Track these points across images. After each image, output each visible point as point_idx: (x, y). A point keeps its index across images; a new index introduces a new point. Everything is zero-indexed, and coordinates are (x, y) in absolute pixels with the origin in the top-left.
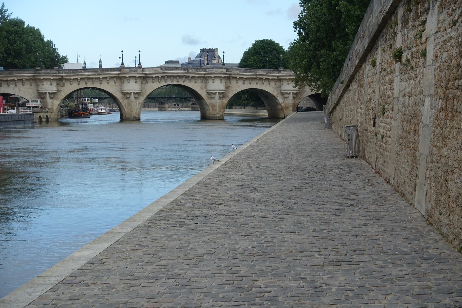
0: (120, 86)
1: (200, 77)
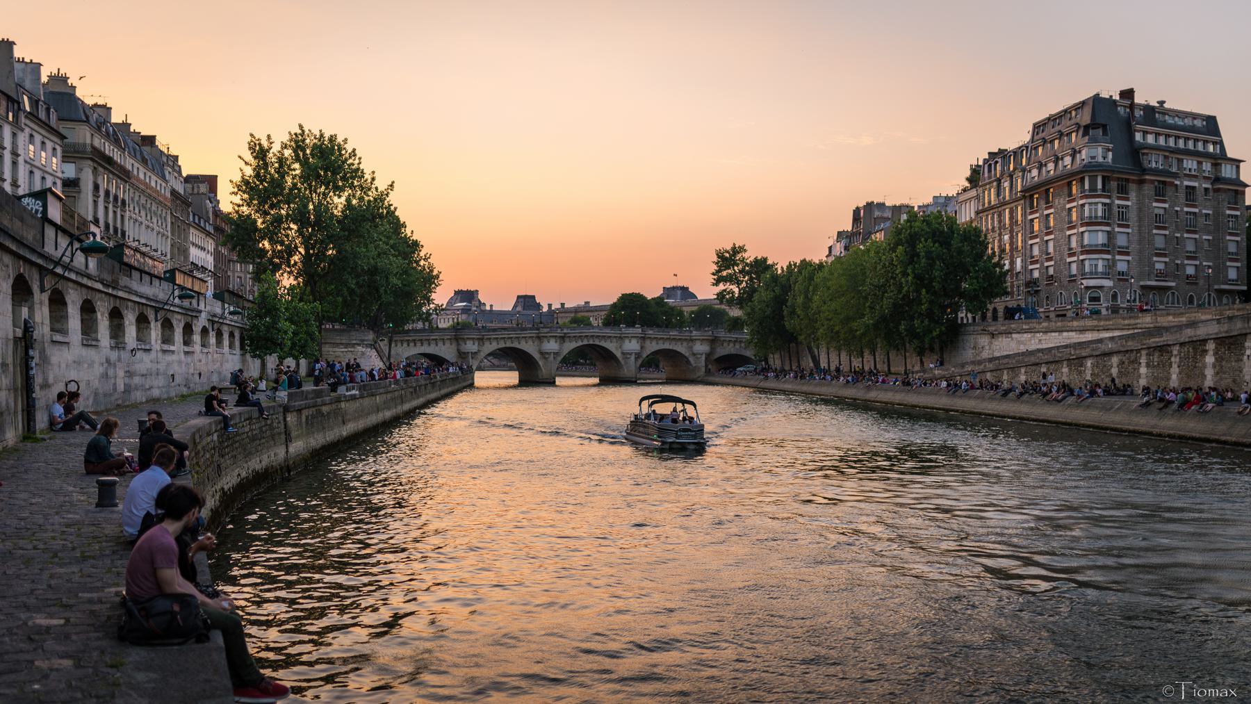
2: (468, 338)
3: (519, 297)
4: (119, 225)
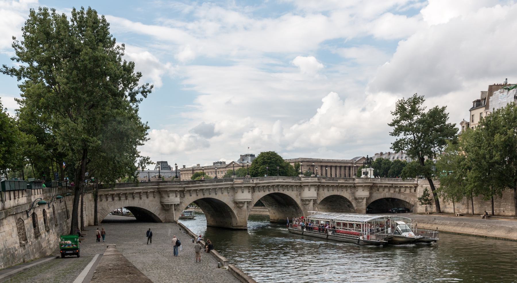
0: (232, 196)
2: (170, 191)
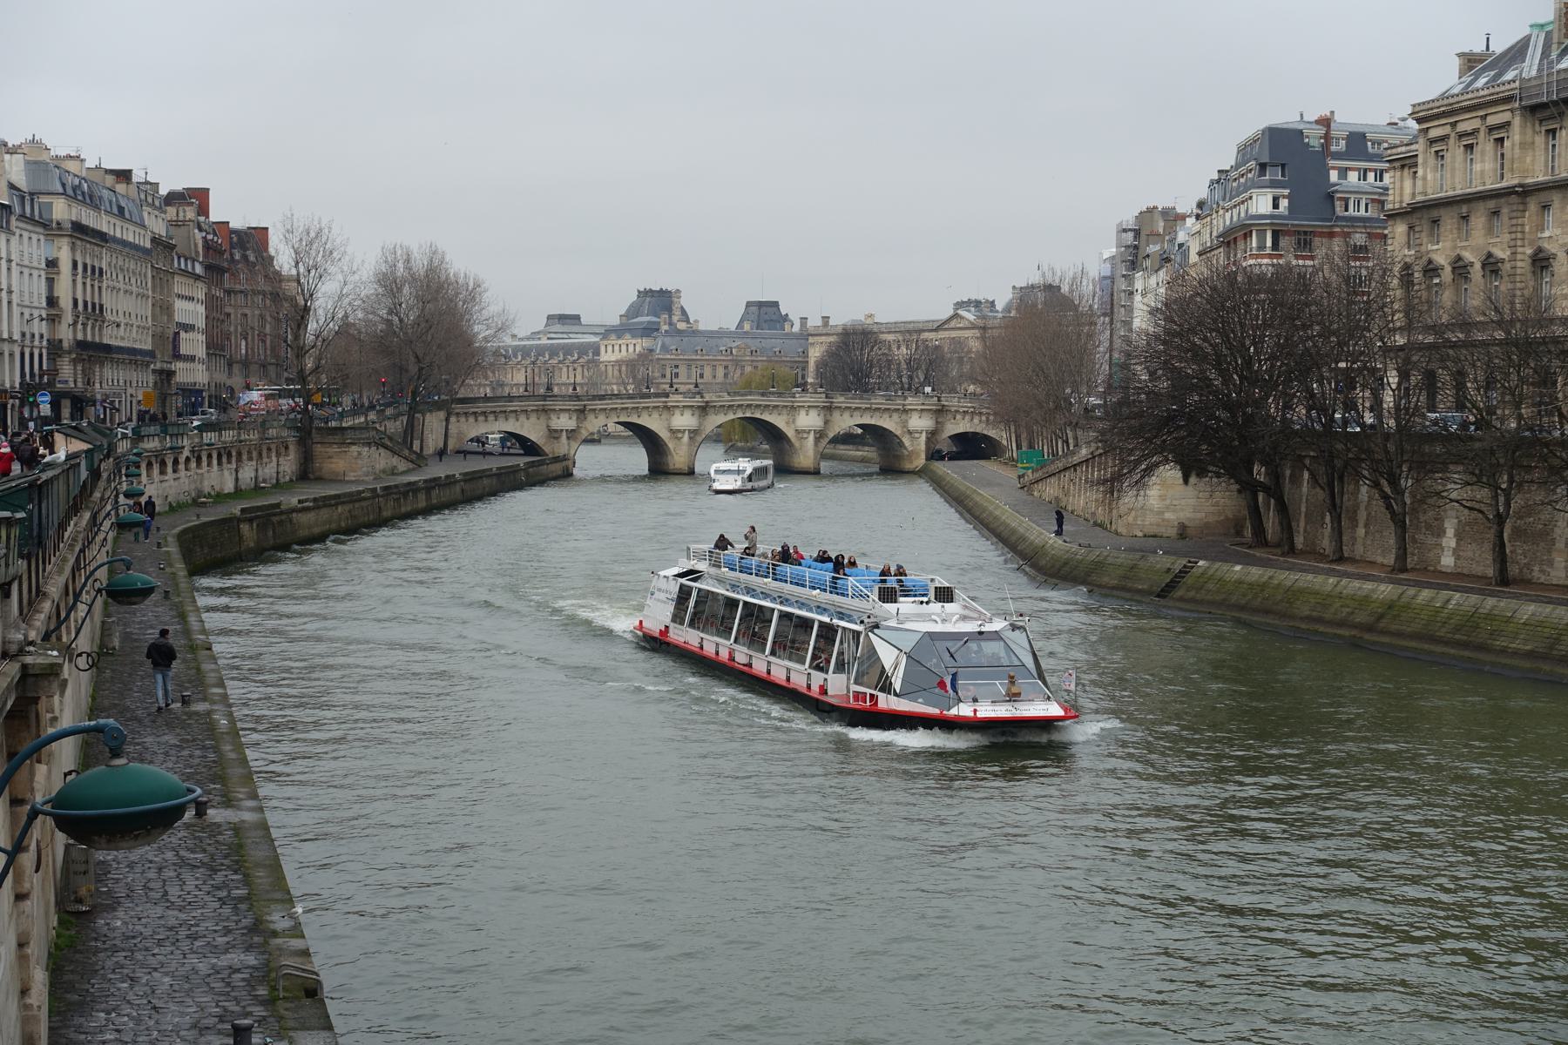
1: (787, 406)
3: (749, 304)
4: (97, 301)
